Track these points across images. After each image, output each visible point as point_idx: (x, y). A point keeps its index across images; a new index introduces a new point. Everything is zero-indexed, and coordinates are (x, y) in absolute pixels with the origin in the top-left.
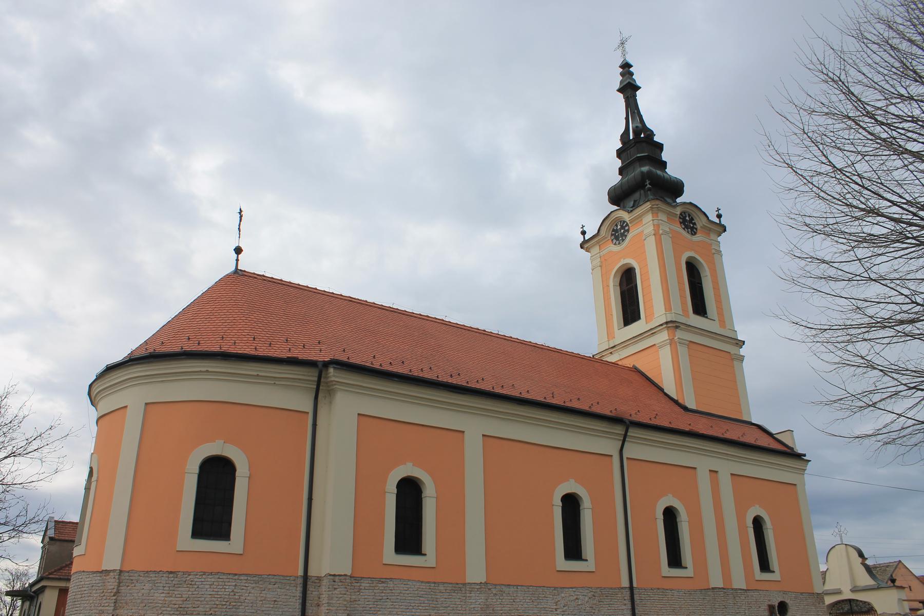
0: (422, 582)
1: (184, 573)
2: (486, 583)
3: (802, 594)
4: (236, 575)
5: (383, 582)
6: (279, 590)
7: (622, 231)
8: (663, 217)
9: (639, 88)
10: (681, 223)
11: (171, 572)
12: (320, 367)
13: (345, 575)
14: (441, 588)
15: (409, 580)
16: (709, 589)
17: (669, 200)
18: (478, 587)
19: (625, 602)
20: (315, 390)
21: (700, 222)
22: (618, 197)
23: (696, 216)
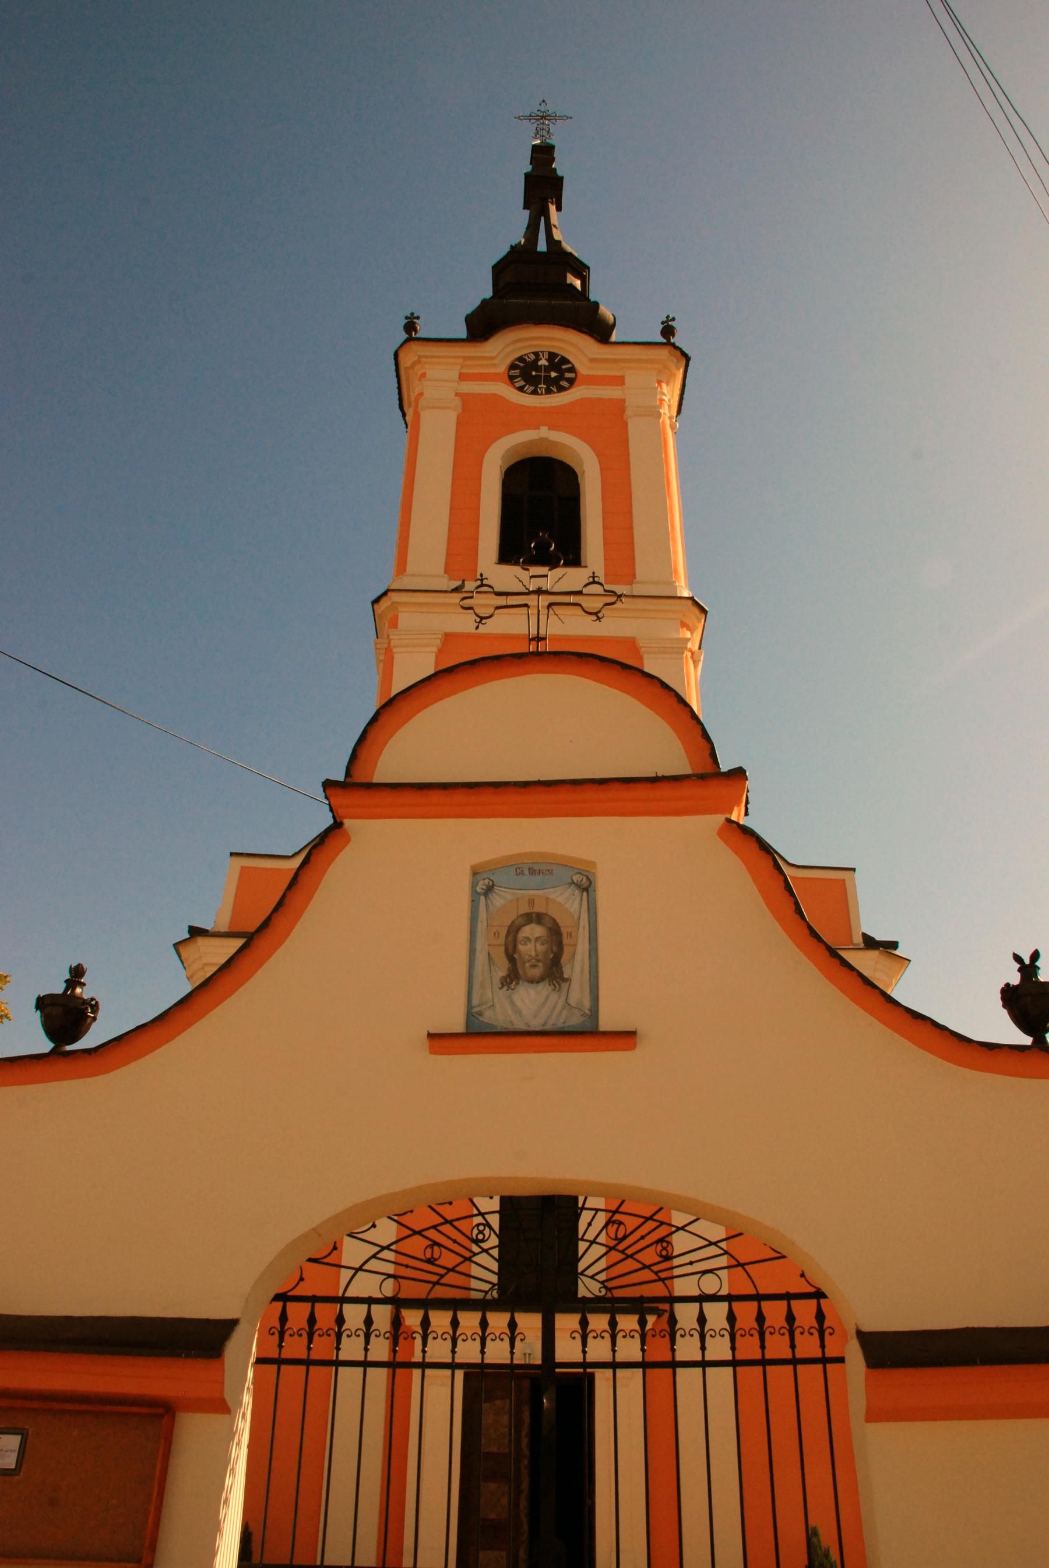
10: (511, 378)
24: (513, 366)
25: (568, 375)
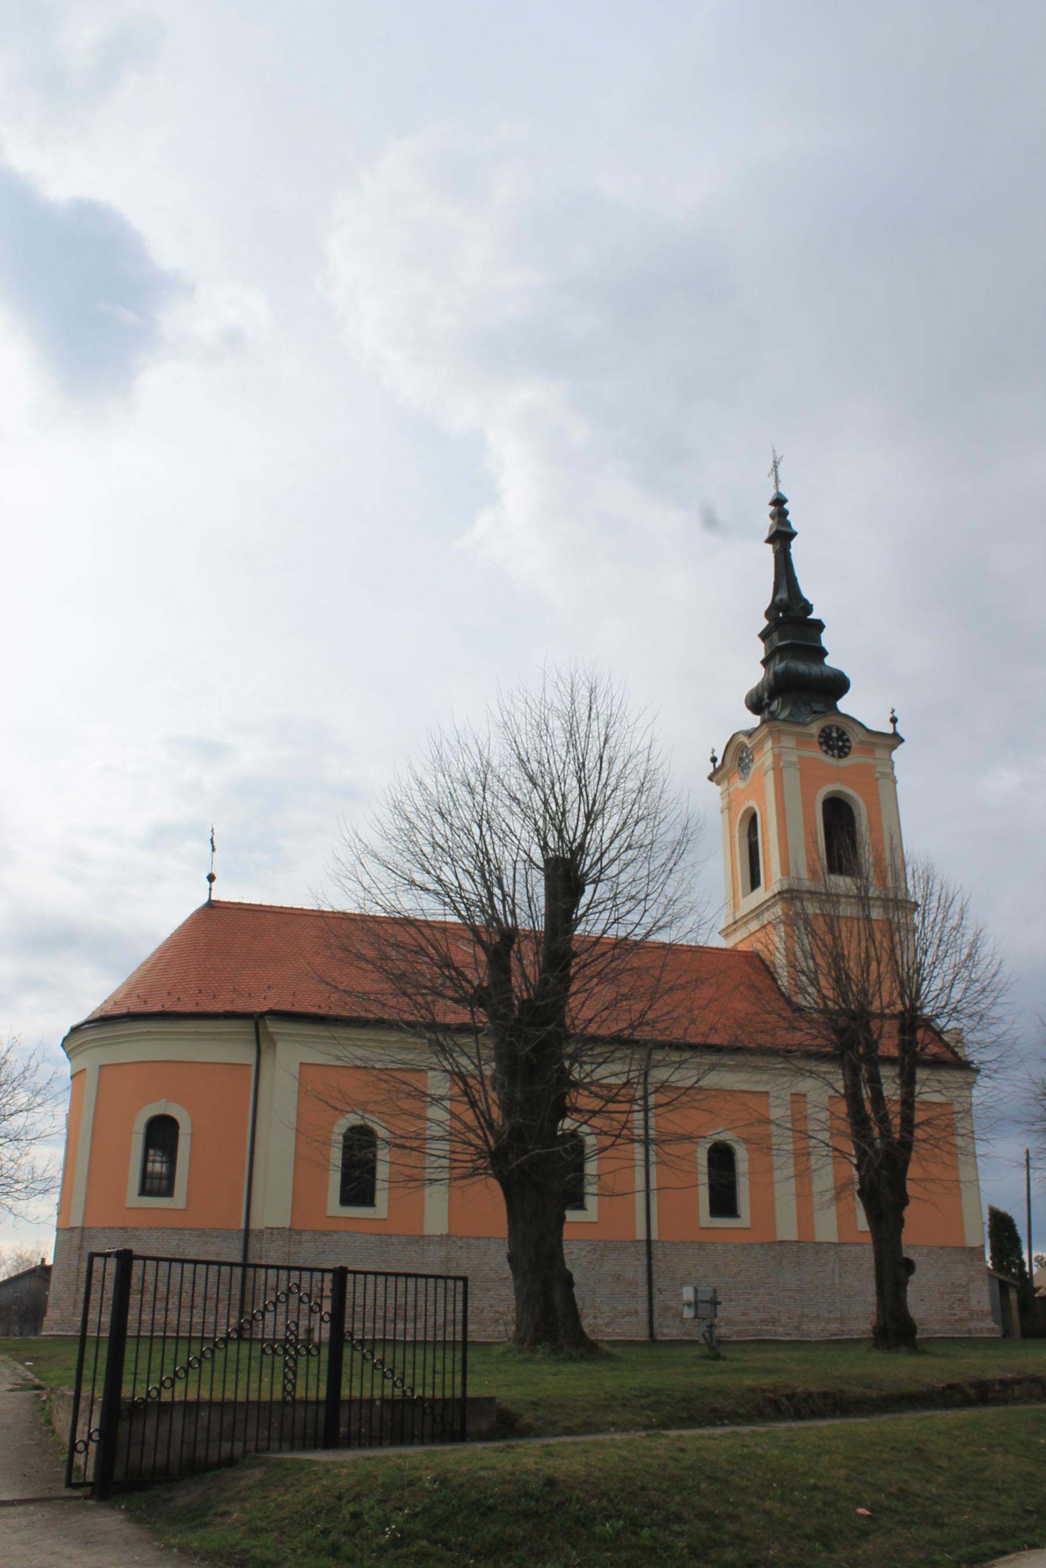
0: (371, 1234)
1: (133, 1228)
2: (448, 1236)
3: (942, 1248)
4: (179, 1229)
5: (326, 1235)
7: (747, 760)
8: (789, 742)
10: (821, 744)
11: (122, 1228)
12: (256, 1018)
13: (284, 1228)
14: (394, 1240)
15: (356, 1233)
17: (817, 707)
18: (438, 1239)
19: (639, 1257)
21: (855, 738)
22: (756, 704)
24: (820, 736)
25: (847, 744)
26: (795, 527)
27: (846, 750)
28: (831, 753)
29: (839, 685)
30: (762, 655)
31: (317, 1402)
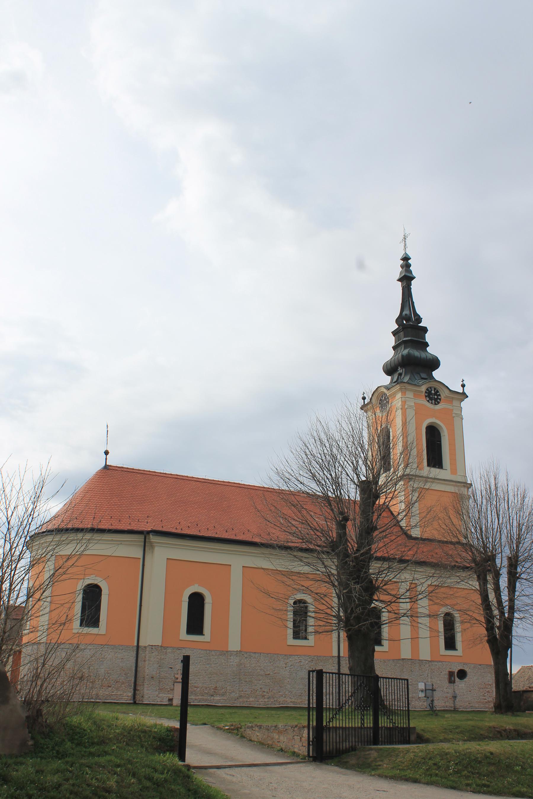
0: (202, 650)
2: (240, 651)
3: (480, 665)
5: (179, 650)
6: (124, 653)
7: (385, 402)
8: (410, 395)
9: (414, 278)
10: (426, 396)
12: (145, 534)
13: (158, 646)
14: (213, 653)
15: (194, 649)
16: (400, 659)
17: (424, 375)
18: (236, 653)
19: (334, 665)
20: (143, 546)
21: (443, 394)
22: (389, 370)
23: (440, 389)
24: (426, 392)
25: (439, 397)
26: (414, 274)
27: (439, 400)
28: (431, 402)
29: (434, 363)
30: (393, 344)
31: (370, 728)
